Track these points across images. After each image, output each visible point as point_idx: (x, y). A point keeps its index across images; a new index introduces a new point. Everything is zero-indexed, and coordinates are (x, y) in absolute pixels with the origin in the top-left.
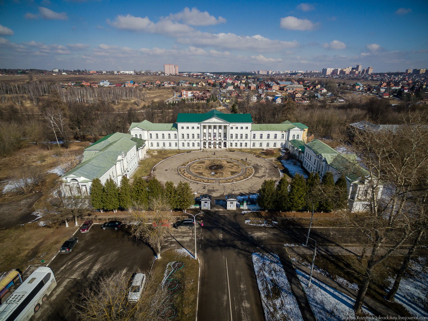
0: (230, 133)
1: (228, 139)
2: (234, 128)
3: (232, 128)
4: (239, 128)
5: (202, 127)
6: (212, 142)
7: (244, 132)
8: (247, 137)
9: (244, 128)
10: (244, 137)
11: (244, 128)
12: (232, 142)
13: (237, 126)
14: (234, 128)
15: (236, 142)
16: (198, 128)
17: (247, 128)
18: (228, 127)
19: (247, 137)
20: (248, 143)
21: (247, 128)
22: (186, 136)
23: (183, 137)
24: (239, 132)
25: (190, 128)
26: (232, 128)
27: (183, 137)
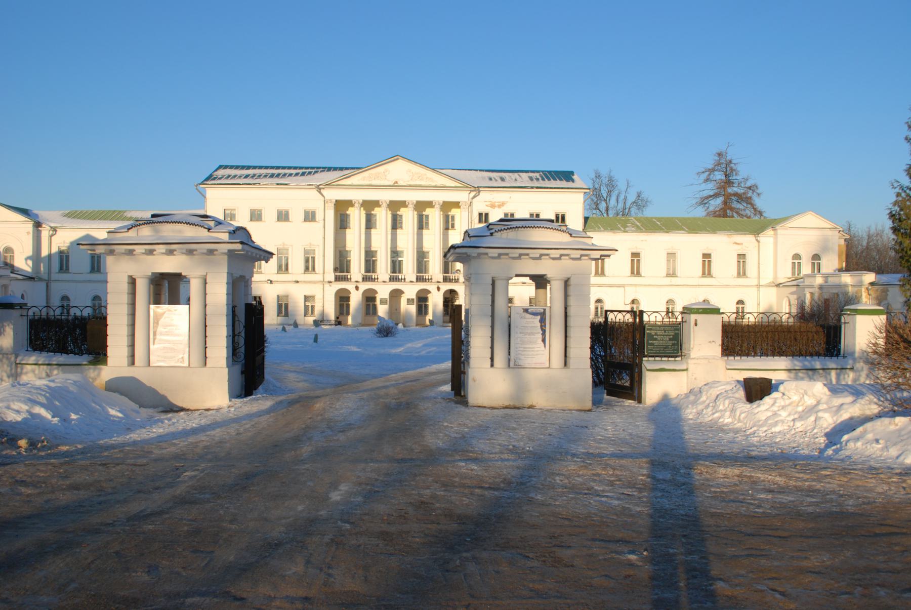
6: (383, 291)
16: (310, 217)
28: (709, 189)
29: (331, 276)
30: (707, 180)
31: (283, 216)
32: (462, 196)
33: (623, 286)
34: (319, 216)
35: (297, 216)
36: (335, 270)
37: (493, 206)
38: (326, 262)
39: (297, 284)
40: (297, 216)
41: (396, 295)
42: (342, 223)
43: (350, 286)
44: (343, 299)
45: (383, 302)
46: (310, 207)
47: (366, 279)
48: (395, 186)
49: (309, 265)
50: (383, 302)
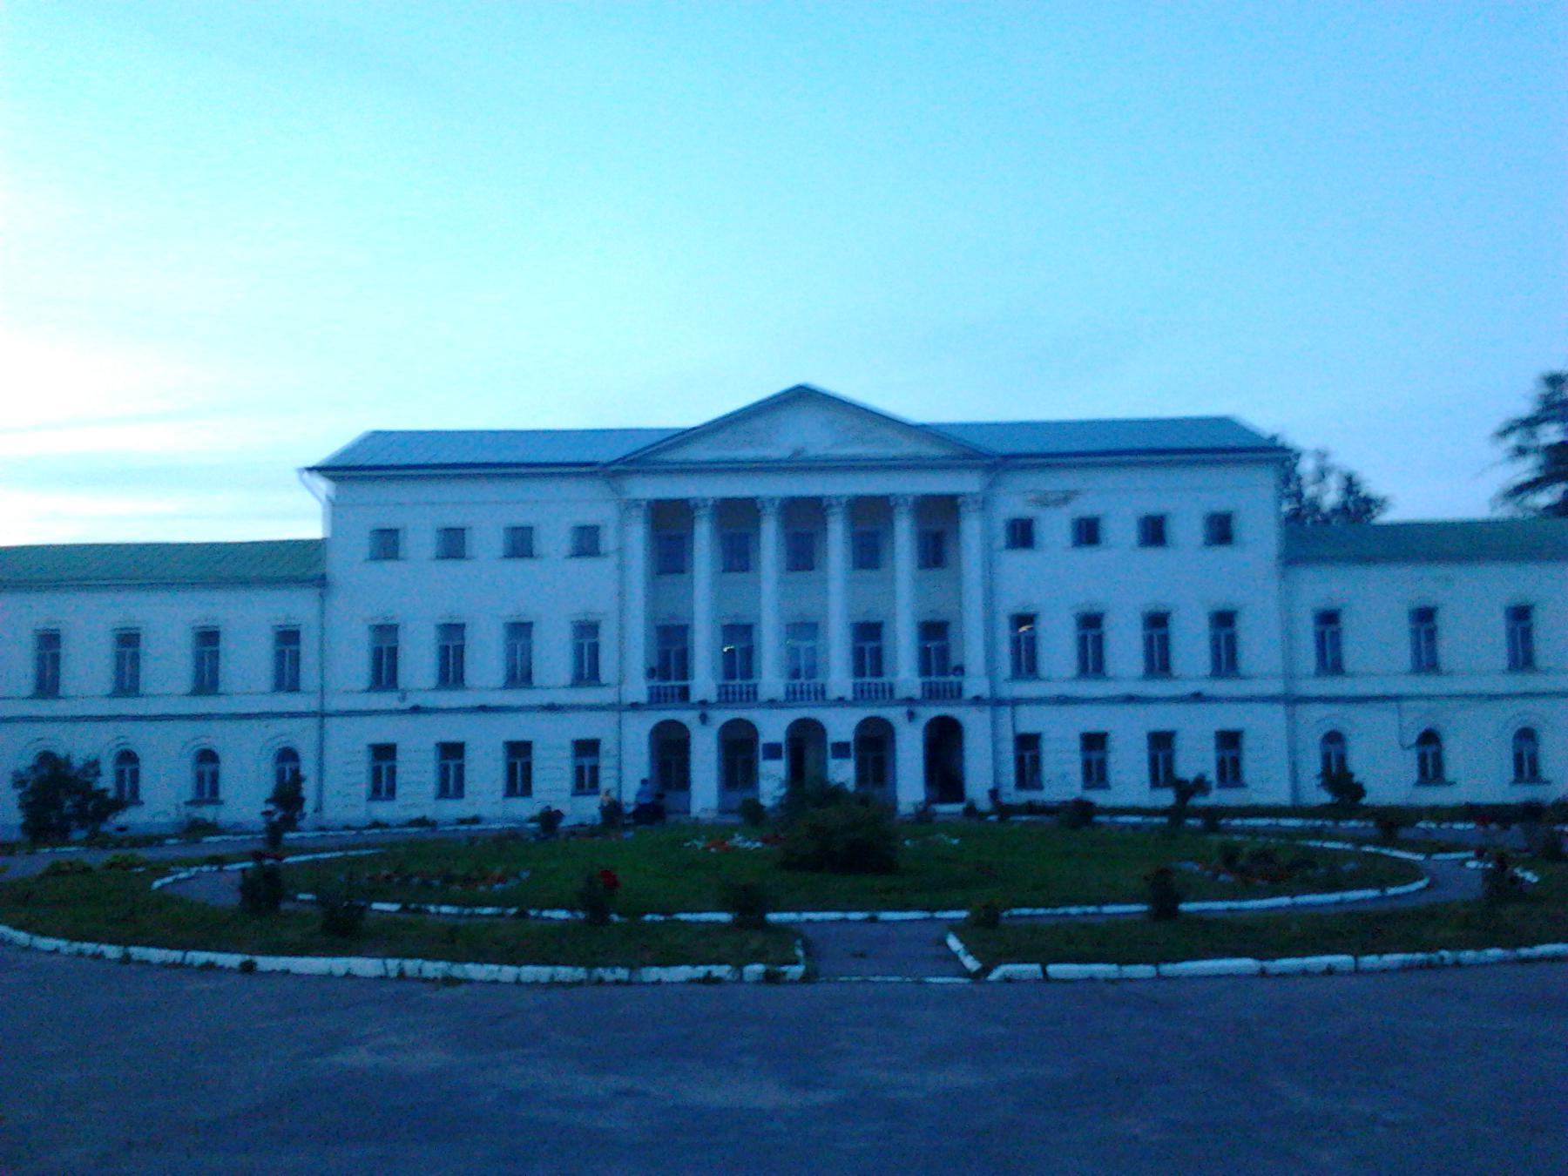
0: (1010, 604)
1: (975, 684)
2: (1055, 527)
3: (1022, 534)
4: (1121, 530)
5: (637, 535)
6: (773, 727)
7: (1189, 580)
8: (1225, 658)
9: (1187, 529)
10: (1191, 647)
11: (1187, 529)
12: (1029, 720)
13: (1085, 507)
14: (1055, 527)
15: (1094, 719)
16: (587, 542)
17: (1221, 530)
18: (972, 529)
19: (1225, 658)
20: (1265, 730)
21: (1221, 530)
22: (418, 662)
23: (385, 670)
24: (1123, 582)
25: (487, 539)
26: (1022, 534)
27: (385, 670)
28: (1526, 469)
29: (638, 689)
30: (1521, 451)
31: (520, 544)
32: (965, 483)
33: (1397, 698)
34: (609, 541)
35: (554, 540)
36: (651, 673)
37: (1043, 502)
38: (628, 663)
39: (556, 716)
40: (554, 540)
41: (805, 738)
42: (670, 554)
43: (688, 717)
44: (670, 749)
45: (773, 751)
46: (588, 517)
47: (726, 697)
48: (798, 465)
49: (587, 671)
50: (773, 751)
